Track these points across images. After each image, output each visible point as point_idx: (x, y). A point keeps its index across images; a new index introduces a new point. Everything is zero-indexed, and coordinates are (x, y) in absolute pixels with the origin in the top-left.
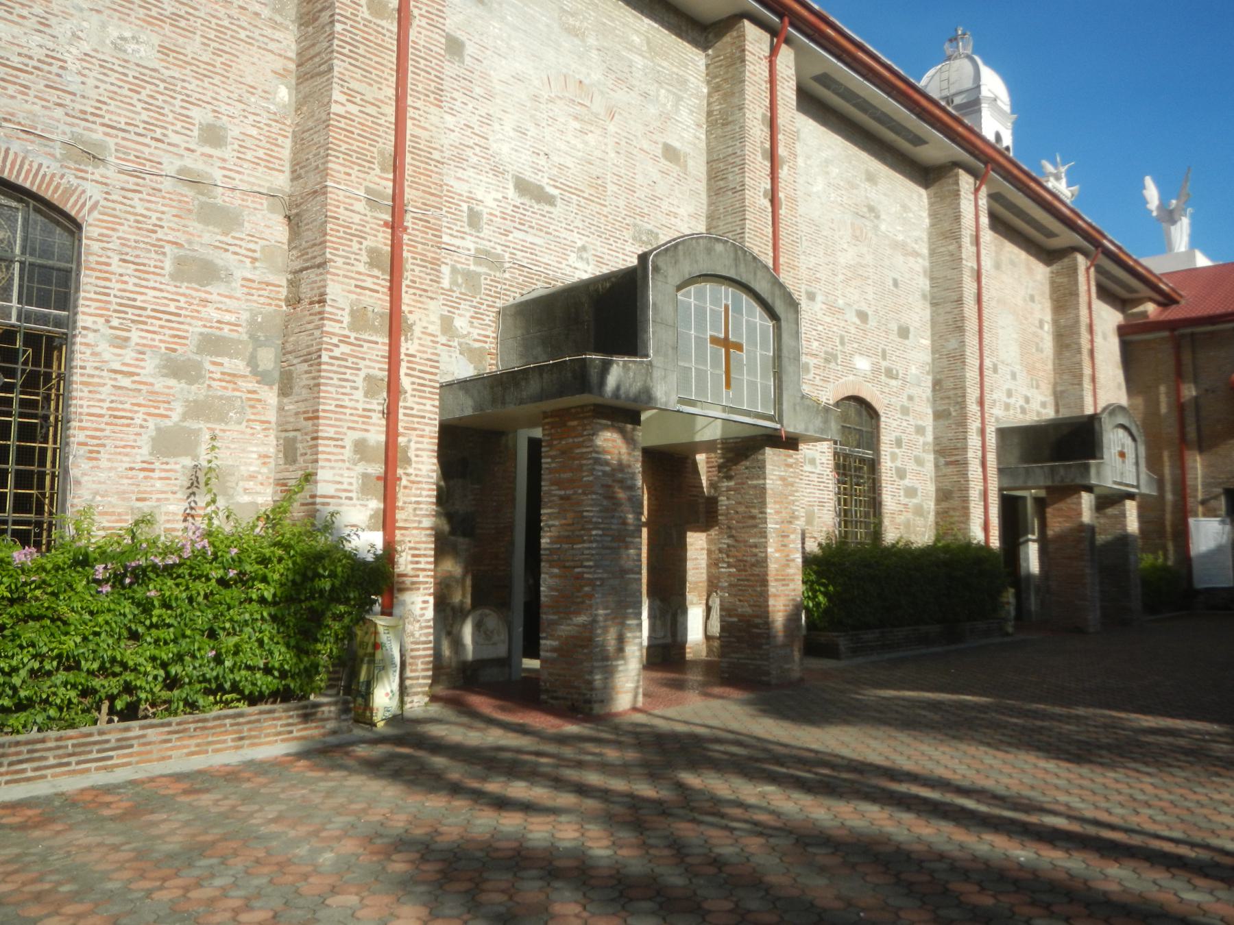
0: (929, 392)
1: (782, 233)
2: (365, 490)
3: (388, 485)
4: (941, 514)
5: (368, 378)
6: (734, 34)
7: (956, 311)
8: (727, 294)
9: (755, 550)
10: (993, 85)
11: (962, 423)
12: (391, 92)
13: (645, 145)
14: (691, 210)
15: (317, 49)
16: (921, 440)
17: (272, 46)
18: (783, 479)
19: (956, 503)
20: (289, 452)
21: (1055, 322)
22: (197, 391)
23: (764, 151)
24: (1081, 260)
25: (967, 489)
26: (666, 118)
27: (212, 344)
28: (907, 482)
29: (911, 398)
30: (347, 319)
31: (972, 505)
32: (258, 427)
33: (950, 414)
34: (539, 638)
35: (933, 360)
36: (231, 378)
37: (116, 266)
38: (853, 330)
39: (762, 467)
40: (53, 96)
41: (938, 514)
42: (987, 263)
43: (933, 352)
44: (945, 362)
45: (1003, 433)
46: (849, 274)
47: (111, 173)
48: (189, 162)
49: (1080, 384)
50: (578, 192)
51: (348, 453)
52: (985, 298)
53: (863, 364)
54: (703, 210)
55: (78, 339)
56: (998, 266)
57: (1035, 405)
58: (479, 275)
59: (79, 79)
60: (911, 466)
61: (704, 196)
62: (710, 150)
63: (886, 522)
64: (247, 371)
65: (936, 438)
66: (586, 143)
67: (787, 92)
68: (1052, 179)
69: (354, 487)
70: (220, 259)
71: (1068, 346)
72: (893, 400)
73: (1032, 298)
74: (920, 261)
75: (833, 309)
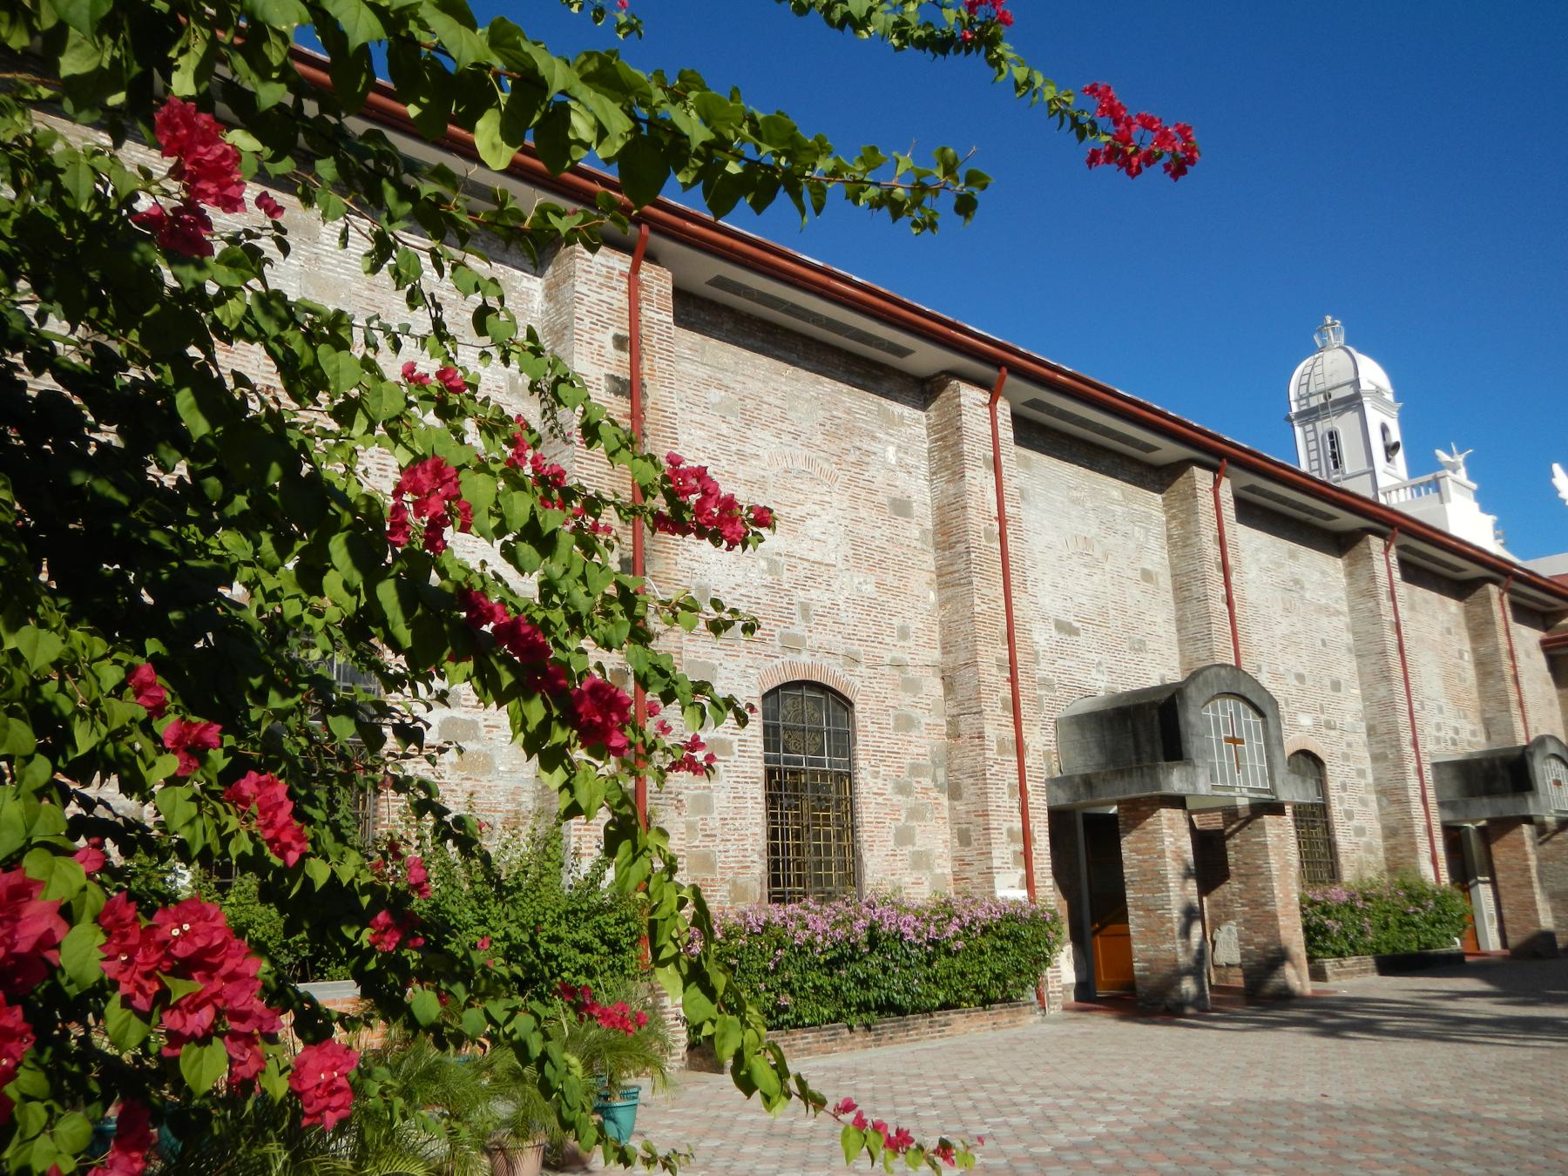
0: (1364, 736)
1: (1239, 627)
2: (1016, 862)
3: (1027, 856)
4: (1391, 850)
5: (1010, 784)
6: (1185, 475)
7: (1382, 662)
8: (1230, 703)
9: (1264, 892)
10: (1372, 374)
11: (1399, 764)
12: (1001, 590)
13: (1130, 573)
14: (1165, 616)
15: (955, 568)
16: (1363, 782)
17: (924, 566)
18: (1278, 836)
19: (1402, 839)
20: (964, 838)
21: (1474, 651)
22: (911, 802)
23: (1217, 563)
24: (1493, 589)
25: (1412, 826)
26: (1141, 548)
27: (916, 770)
28: (1355, 823)
29: (1349, 745)
30: (995, 748)
31: (1418, 840)
32: (941, 822)
33: (1386, 756)
34: (1131, 963)
35: (1365, 707)
36: (926, 790)
37: (871, 728)
38: (1294, 692)
39: (1263, 828)
40: (836, 628)
41: (1387, 850)
42: (1404, 614)
43: (1365, 699)
44: (1376, 709)
45: (1436, 766)
46: (1285, 643)
47: (861, 669)
48: (897, 654)
49: (1508, 710)
50: (1090, 622)
51: (1005, 838)
52: (1406, 647)
53: (1305, 720)
54: (1173, 615)
55: (859, 776)
56: (1412, 608)
57: (1465, 735)
58: (1041, 696)
59: (845, 614)
60: (1357, 807)
61: (1172, 603)
62: (1173, 566)
63: (1342, 860)
64: (931, 785)
65: (1376, 779)
66: (1092, 583)
67: (1229, 510)
68: (1449, 473)
69: (1010, 860)
70: (917, 713)
71: (1490, 673)
72: (1335, 748)
73: (1449, 631)
74: (1342, 618)
75: (1276, 676)
